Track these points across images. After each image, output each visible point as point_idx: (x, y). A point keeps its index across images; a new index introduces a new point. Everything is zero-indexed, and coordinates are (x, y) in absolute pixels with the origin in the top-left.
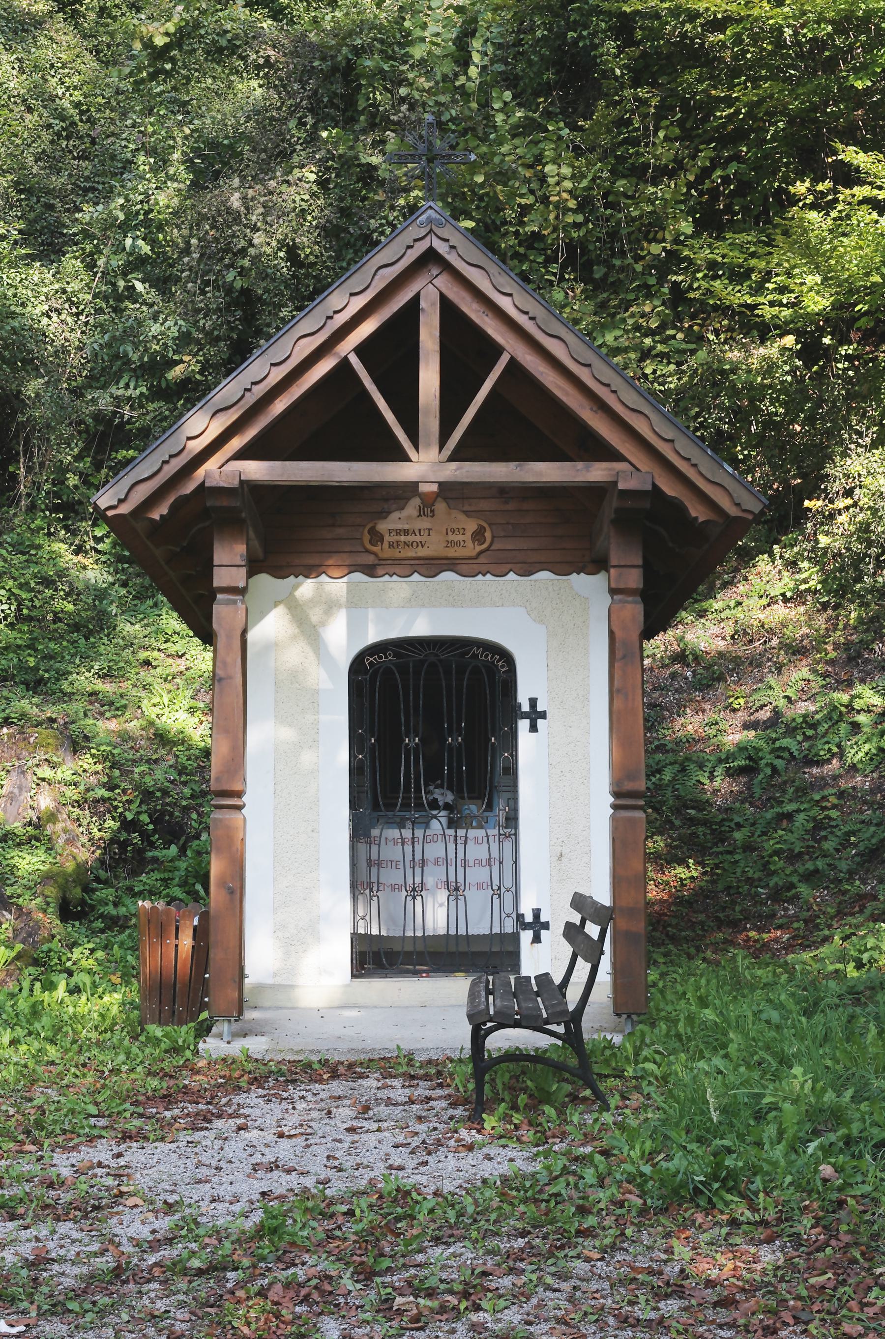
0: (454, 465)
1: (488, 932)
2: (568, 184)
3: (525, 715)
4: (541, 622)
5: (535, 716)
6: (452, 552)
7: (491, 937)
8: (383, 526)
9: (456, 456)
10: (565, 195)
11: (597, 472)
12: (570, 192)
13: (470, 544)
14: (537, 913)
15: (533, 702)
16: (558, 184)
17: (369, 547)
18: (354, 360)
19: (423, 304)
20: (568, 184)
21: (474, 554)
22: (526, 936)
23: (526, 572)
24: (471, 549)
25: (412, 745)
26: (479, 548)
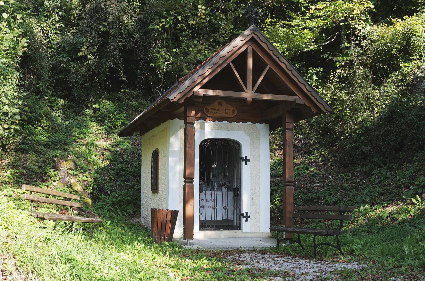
0: (256, 94)
1: (210, 219)
2: (203, 11)
3: (244, 160)
4: (248, 135)
5: (247, 161)
6: (227, 116)
7: (211, 221)
8: (209, 108)
9: (256, 92)
10: (202, 14)
11: (291, 98)
12: (203, 14)
13: (231, 113)
14: (247, 213)
15: (246, 157)
16: (201, 11)
17: (205, 113)
18: (231, 64)
19: (248, 50)
20: (203, 11)
21: (232, 116)
22: (244, 219)
23: (245, 122)
24: (232, 115)
25: (214, 167)
26: (234, 115)
